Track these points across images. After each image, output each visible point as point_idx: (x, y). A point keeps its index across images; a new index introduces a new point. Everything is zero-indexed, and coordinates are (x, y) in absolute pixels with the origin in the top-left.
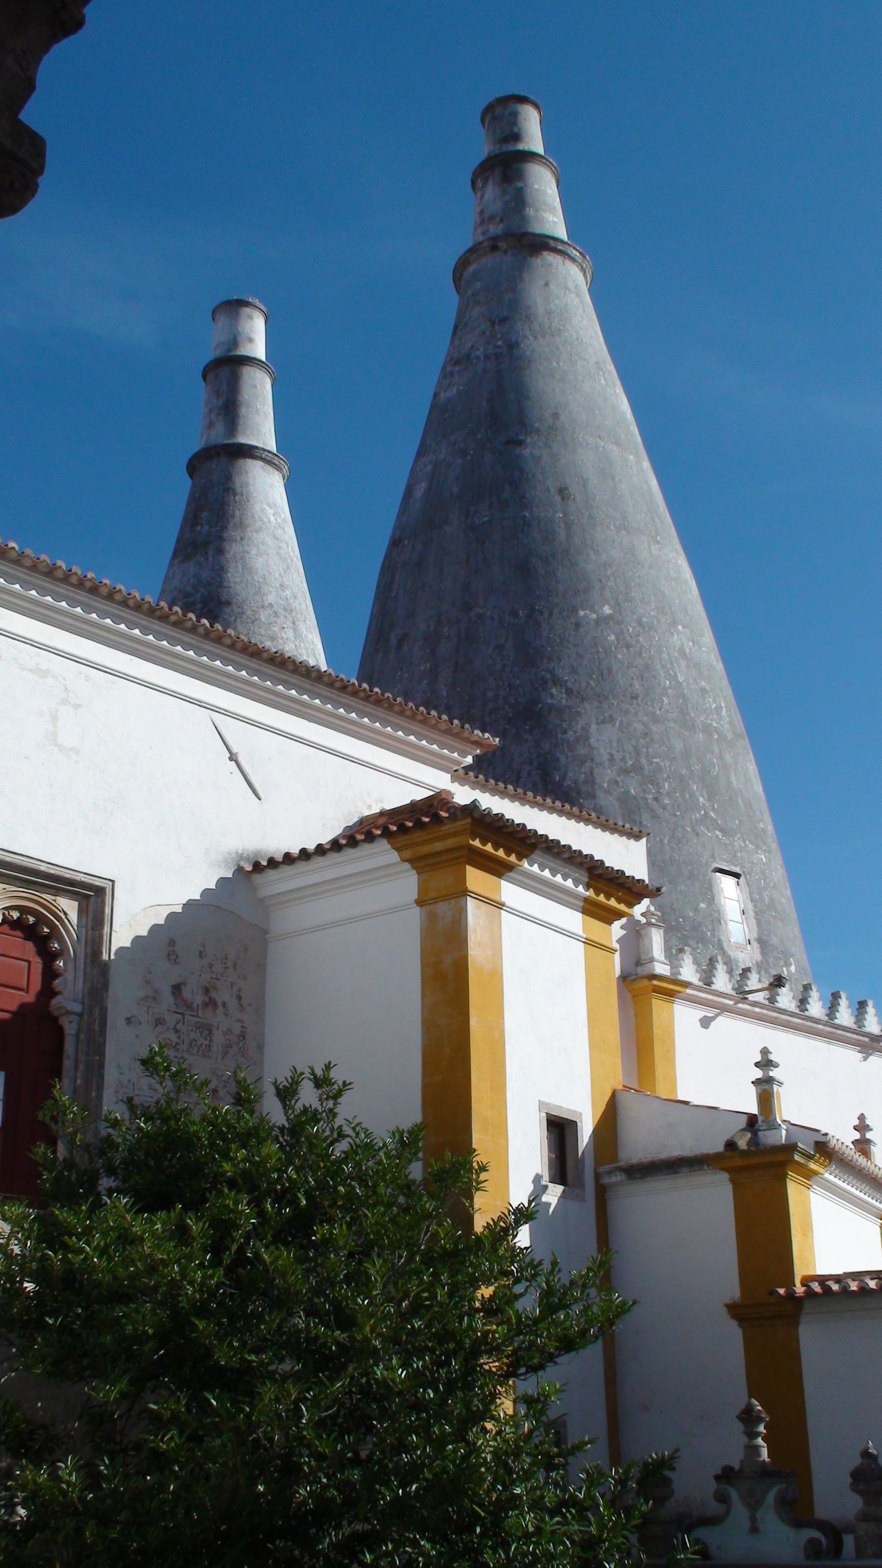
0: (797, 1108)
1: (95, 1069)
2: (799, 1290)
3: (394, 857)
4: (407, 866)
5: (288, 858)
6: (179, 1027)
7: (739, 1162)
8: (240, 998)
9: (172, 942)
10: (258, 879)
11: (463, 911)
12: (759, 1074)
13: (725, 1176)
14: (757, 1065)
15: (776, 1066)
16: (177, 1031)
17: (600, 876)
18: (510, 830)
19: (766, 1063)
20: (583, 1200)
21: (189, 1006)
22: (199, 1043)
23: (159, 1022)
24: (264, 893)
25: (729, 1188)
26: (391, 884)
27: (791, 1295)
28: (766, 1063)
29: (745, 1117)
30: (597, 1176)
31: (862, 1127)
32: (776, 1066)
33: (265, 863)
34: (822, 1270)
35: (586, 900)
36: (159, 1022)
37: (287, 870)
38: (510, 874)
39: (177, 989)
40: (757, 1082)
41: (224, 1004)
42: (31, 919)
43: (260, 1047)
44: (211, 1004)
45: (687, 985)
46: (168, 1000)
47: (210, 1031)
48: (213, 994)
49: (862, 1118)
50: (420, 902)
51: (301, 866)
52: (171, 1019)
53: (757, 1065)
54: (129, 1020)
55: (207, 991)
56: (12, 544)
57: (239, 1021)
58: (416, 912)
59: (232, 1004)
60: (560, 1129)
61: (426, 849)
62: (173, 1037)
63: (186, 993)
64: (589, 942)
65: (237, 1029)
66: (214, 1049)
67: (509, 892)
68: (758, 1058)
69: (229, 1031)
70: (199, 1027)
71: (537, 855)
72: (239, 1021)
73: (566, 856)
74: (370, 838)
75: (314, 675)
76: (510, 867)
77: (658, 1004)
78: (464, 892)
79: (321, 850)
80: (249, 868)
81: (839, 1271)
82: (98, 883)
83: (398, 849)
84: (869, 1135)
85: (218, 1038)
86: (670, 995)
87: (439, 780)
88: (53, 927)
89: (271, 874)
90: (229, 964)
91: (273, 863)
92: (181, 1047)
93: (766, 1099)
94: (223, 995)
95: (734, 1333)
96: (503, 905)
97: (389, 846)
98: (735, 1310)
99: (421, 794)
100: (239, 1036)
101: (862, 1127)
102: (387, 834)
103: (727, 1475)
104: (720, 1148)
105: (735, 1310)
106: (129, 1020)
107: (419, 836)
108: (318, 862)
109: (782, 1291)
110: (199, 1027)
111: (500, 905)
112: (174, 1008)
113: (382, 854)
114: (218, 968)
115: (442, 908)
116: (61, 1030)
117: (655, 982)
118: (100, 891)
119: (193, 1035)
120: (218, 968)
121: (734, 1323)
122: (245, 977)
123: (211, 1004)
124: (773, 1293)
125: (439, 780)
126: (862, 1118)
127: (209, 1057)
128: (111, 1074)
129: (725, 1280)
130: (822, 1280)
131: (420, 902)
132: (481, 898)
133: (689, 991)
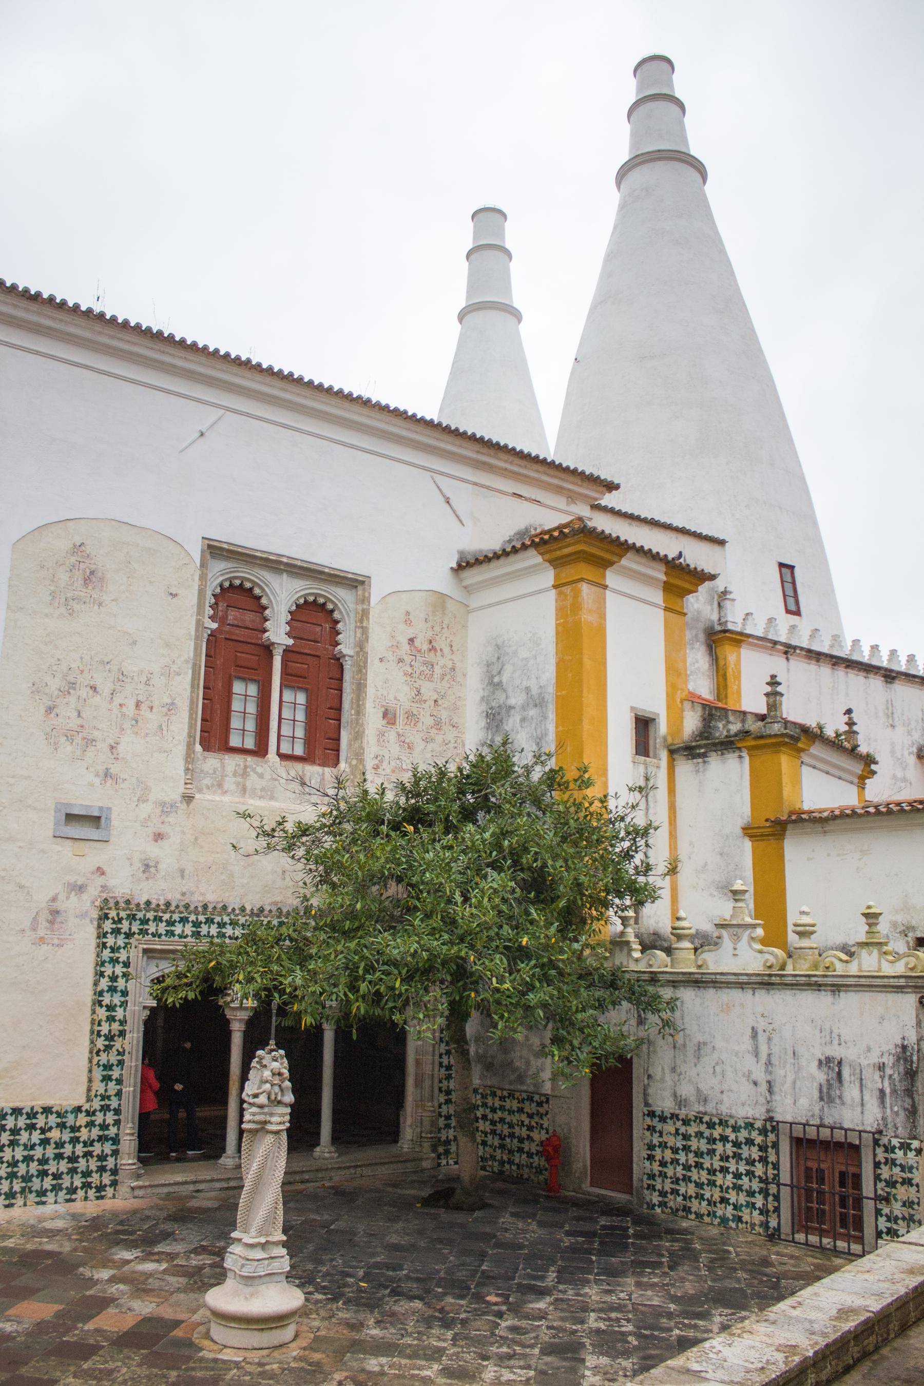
0: (795, 710)
1: (360, 687)
3: (539, 559)
4: (548, 564)
7: (753, 743)
9: (408, 613)
11: (580, 591)
12: (768, 689)
14: (767, 684)
15: (779, 684)
16: (411, 666)
19: (774, 682)
20: (658, 767)
21: (419, 651)
23: (401, 660)
25: (747, 759)
28: (774, 682)
32: (779, 684)
33: (464, 564)
34: (806, 807)
35: (665, 582)
39: (411, 641)
40: (767, 695)
41: (441, 650)
43: (464, 675)
44: (433, 649)
46: (405, 647)
48: (434, 644)
50: (555, 587)
52: (408, 659)
53: (767, 684)
54: (381, 660)
55: (431, 642)
57: (451, 660)
58: (553, 593)
59: (446, 650)
60: (643, 724)
61: (559, 553)
62: (410, 670)
63: (417, 643)
65: (450, 665)
66: (435, 676)
67: (612, 578)
68: (769, 680)
69: (444, 666)
70: (425, 663)
71: (630, 555)
72: (451, 660)
74: (524, 547)
76: (611, 564)
83: (542, 554)
84: (855, 728)
85: (438, 671)
87: (583, 510)
88: (336, 605)
93: (773, 706)
94: (440, 644)
96: (607, 586)
97: (535, 552)
98: (749, 831)
102: (534, 544)
105: (749, 831)
106: (381, 660)
107: (554, 546)
111: (605, 587)
112: (409, 652)
113: (533, 558)
114: (437, 629)
115: (567, 590)
116: (342, 666)
117: (727, 634)
118: (363, 583)
119: (421, 668)
120: (437, 629)
123: (433, 649)
125: (583, 510)
128: (370, 691)
131: (555, 587)
132: (590, 582)
133: (750, 640)
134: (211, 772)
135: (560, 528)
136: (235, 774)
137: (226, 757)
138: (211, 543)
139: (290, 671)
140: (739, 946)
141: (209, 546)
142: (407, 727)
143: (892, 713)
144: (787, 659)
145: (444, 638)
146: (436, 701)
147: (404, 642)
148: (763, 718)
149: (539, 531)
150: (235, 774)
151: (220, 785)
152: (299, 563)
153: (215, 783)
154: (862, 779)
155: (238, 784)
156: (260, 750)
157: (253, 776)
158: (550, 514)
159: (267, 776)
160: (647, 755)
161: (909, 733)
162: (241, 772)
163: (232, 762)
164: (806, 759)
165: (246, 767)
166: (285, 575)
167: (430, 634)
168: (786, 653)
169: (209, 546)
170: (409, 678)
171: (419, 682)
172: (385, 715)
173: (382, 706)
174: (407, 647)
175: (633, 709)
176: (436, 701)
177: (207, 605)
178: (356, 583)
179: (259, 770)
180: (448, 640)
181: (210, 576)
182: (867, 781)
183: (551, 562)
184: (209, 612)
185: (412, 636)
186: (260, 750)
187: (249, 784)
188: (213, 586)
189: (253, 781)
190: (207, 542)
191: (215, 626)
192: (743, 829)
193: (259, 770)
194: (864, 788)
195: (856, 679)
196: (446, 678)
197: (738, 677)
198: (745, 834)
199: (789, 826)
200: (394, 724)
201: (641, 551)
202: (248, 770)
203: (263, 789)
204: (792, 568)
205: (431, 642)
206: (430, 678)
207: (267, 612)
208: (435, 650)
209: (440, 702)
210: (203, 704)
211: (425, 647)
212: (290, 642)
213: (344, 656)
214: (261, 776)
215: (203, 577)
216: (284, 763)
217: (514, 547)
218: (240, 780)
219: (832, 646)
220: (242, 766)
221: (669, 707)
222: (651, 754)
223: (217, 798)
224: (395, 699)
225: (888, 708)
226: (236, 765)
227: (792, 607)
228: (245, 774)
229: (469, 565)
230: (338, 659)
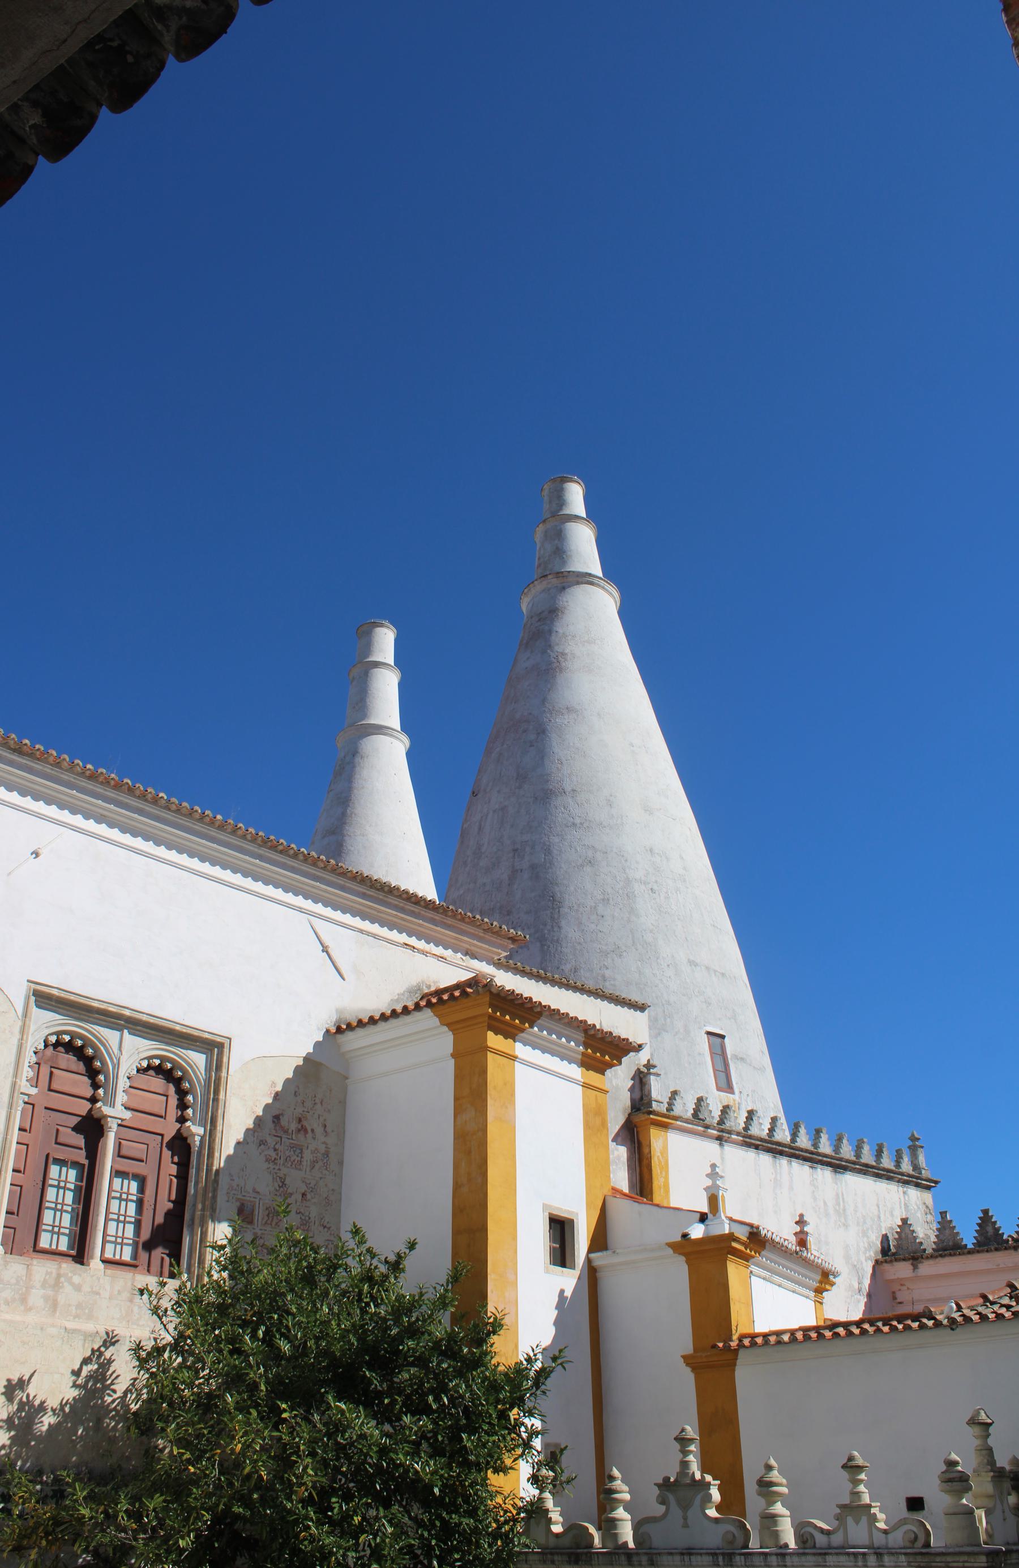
0: (740, 1208)
2: (734, 1344)
3: (436, 1021)
4: (446, 1028)
5: (361, 1023)
6: (277, 1147)
8: (325, 1126)
10: (340, 1038)
13: (683, 1258)
14: (707, 1175)
16: (275, 1150)
17: (593, 1036)
18: (520, 1002)
19: (713, 1174)
21: (286, 1132)
22: (292, 1159)
24: (346, 1048)
25: (685, 1268)
26: (434, 1042)
27: (727, 1348)
29: (698, 1215)
30: (588, 1261)
31: (801, 1222)
33: (344, 1027)
36: (262, 1143)
37: (360, 1032)
38: (522, 1035)
41: (313, 1131)
42: (169, 1066)
43: (341, 1163)
45: (676, 1118)
46: (270, 1124)
47: (302, 1150)
48: (305, 1123)
49: (801, 1216)
50: (453, 1055)
51: (371, 1029)
52: (271, 1141)
53: (707, 1175)
55: (300, 1120)
56: (161, 795)
57: (324, 1143)
59: (319, 1130)
62: (273, 1154)
63: (284, 1122)
64: (586, 1086)
65: (322, 1148)
66: (304, 1163)
70: (292, 1147)
72: (324, 1143)
73: (566, 1020)
75: (386, 889)
77: (654, 1133)
78: (485, 1049)
79: (384, 1017)
80: (333, 1030)
81: (765, 1329)
82: (219, 1039)
85: (308, 1156)
86: (665, 1126)
87: (486, 969)
89: (350, 1035)
90: (317, 1101)
91: (350, 1027)
92: (278, 1161)
95: (688, 1376)
99: (465, 976)
100: (323, 1154)
101: (801, 1222)
102: (429, 1004)
103: (666, 1485)
104: (679, 1239)
108: (382, 1025)
109: (721, 1345)
110: (292, 1147)
111: (513, 1058)
112: (274, 1132)
113: (427, 1019)
118: (221, 1046)
119: (287, 1153)
121: (689, 1369)
122: (329, 1111)
124: (714, 1346)
126: (801, 1216)
127: (300, 1170)
129: (680, 1336)
130: (753, 1336)
133: (679, 1123)
134: (13, 1281)
135: (457, 986)
136: (44, 1284)
137: (35, 1262)
138: (39, 987)
139: (124, 1152)
140: (690, 1513)
141: (37, 994)
142: (268, 1228)
143: (844, 1210)
144: (721, 1145)
145: (316, 1116)
146: (304, 1195)
147: (270, 1119)
148: (703, 1218)
149: (433, 989)
150: (44, 1284)
151: (24, 1300)
152: (145, 1018)
153: (17, 1296)
154: (819, 1291)
155: (46, 1299)
156: (79, 1254)
157: (68, 1288)
158: (445, 968)
159: (86, 1288)
160: (563, 1265)
161: (865, 1233)
162: (52, 1282)
163: (43, 1269)
164: (753, 1268)
165: (59, 1276)
166: (126, 1031)
167: (299, 1110)
168: (719, 1139)
169: (37, 994)
170: (271, 1165)
171: (284, 1170)
172: (240, 1211)
173: (238, 1200)
174: (272, 1126)
175: (545, 1206)
176: (304, 1195)
177: (27, 1064)
178: (214, 1048)
179: (76, 1279)
180: (321, 1119)
181: (33, 1028)
182: (825, 1294)
183: (448, 1025)
184: (27, 1072)
185: (277, 1113)
186: (79, 1254)
187: (61, 1299)
188: (35, 1040)
189: (67, 1295)
190: (33, 986)
191: (34, 1091)
192: (683, 1357)
193: (76, 1279)
194: (821, 1303)
195: (800, 1170)
196: (317, 1166)
197: (666, 1167)
198: (688, 1364)
199: (742, 1353)
200: (251, 1222)
201: (555, 1015)
202: (62, 1279)
203: (79, 1306)
204: (723, 1037)
205: (300, 1120)
206: (298, 1165)
207: (101, 1077)
208: (306, 1131)
209: (309, 1196)
210: (10, 1191)
211: (294, 1126)
212: (128, 1115)
213: (194, 1135)
214: (78, 1288)
215: (23, 1030)
216: (109, 1272)
217: (405, 1008)
218: (50, 1292)
219: (772, 1130)
220: (54, 1275)
221: (589, 1205)
222: (568, 1264)
223: (18, 1318)
224: (255, 1191)
225: (838, 1204)
226: (47, 1273)
227: (723, 1083)
228: (57, 1285)
229: (350, 1027)
230: (186, 1139)
